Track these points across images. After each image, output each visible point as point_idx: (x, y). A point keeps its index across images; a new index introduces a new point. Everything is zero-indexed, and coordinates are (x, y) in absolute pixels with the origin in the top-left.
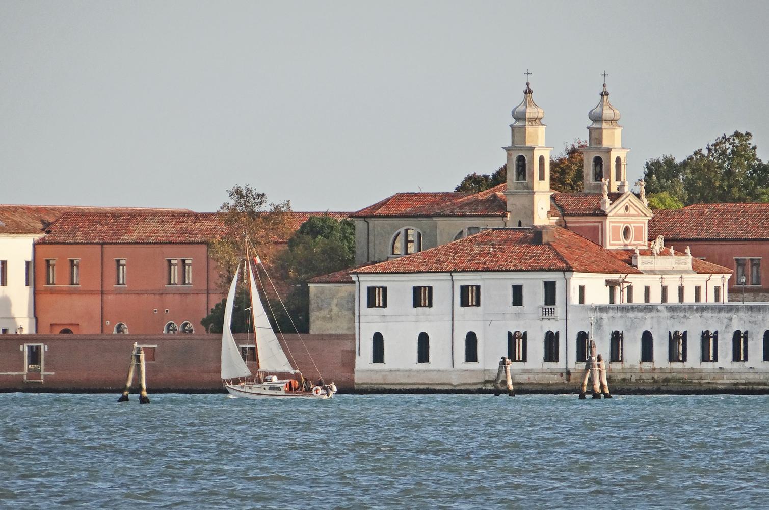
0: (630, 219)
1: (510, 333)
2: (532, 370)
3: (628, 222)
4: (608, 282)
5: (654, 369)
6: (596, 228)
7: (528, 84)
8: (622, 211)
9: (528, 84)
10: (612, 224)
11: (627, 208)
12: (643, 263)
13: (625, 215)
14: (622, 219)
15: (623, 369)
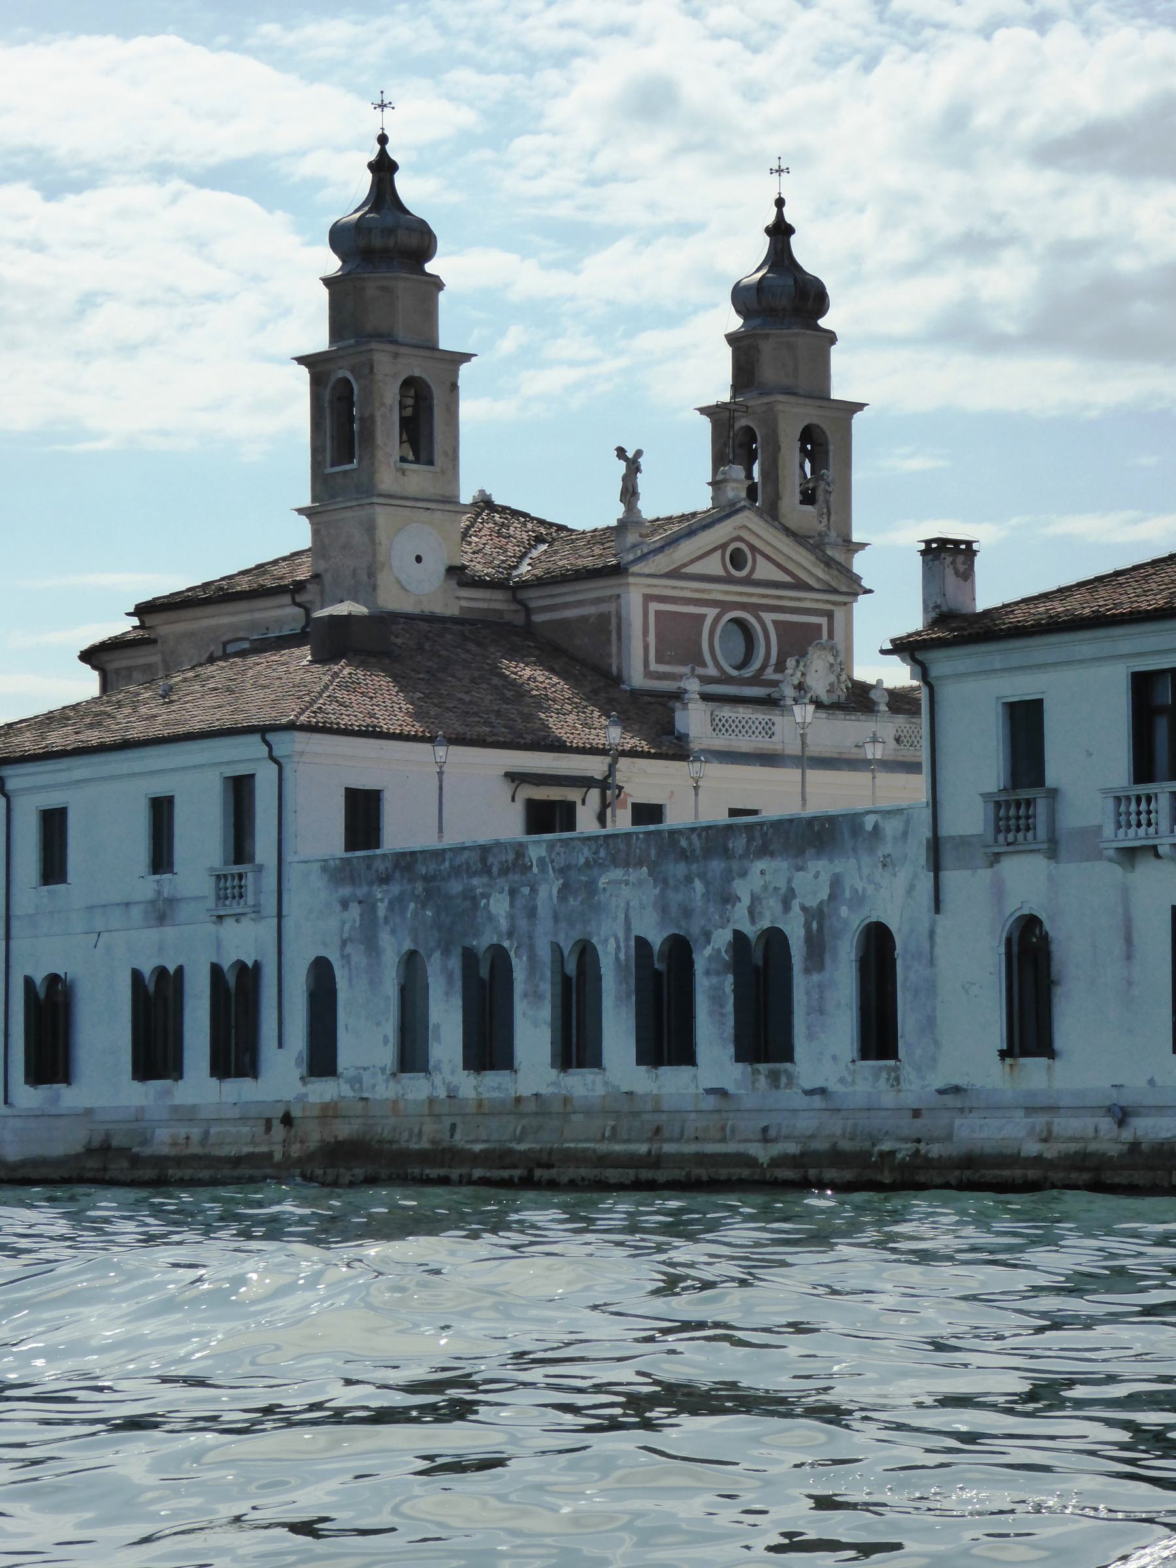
0: (754, 596)
1: (136, 975)
2: (194, 1108)
3: (743, 606)
4: (516, 778)
5: (518, 1100)
6: (604, 618)
7: (383, 139)
8: (714, 566)
9: (383, 139)
10: (654, 606)
11: (737, 559)
12: (717, 726)
13: (729, 580)
14: (718, 592)
15: (431, 1101)
